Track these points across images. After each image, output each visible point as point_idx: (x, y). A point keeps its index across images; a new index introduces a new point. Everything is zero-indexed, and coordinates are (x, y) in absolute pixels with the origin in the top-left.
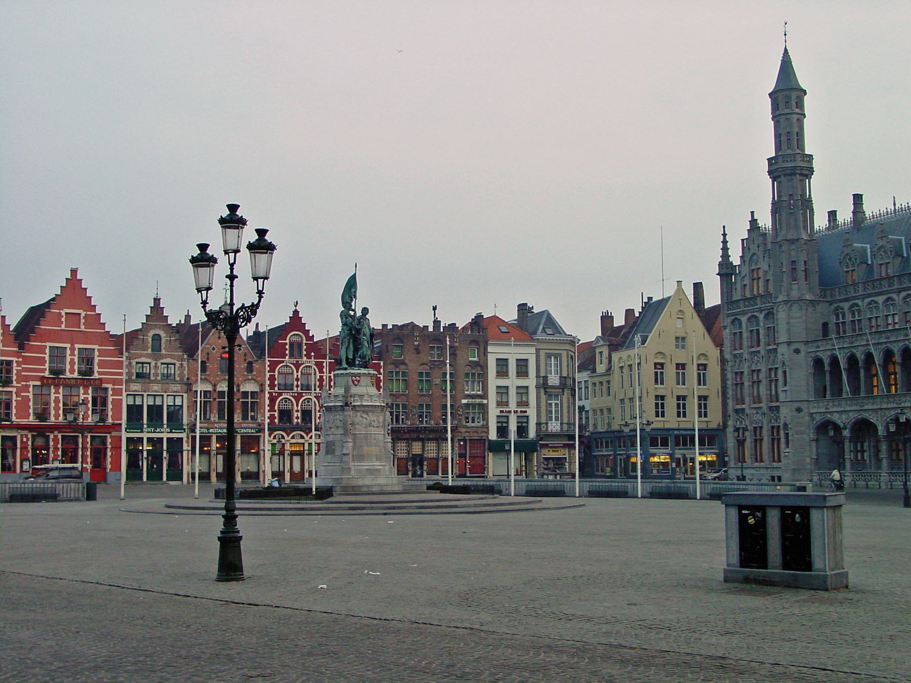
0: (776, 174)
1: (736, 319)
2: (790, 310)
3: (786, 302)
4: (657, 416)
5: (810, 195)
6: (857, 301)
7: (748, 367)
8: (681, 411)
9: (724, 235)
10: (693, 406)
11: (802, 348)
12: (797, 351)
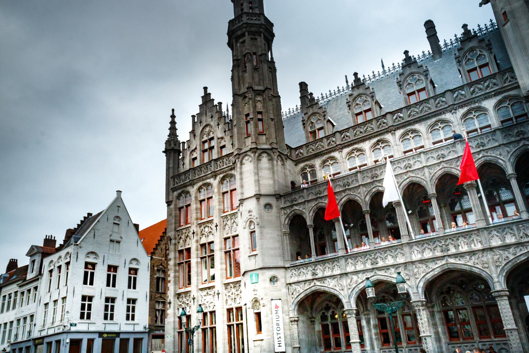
0: (239, 33)
1: (183, 192)
2: (259, 159)
3: (254, 150)
4: (82, 317)
5: (272, 58)
6: (333, 154)
7: (197, 241)
8: (109, 315)
9: (173, 117)
10: (120, 308)
11: (272, 201)
12: (268, 206)
